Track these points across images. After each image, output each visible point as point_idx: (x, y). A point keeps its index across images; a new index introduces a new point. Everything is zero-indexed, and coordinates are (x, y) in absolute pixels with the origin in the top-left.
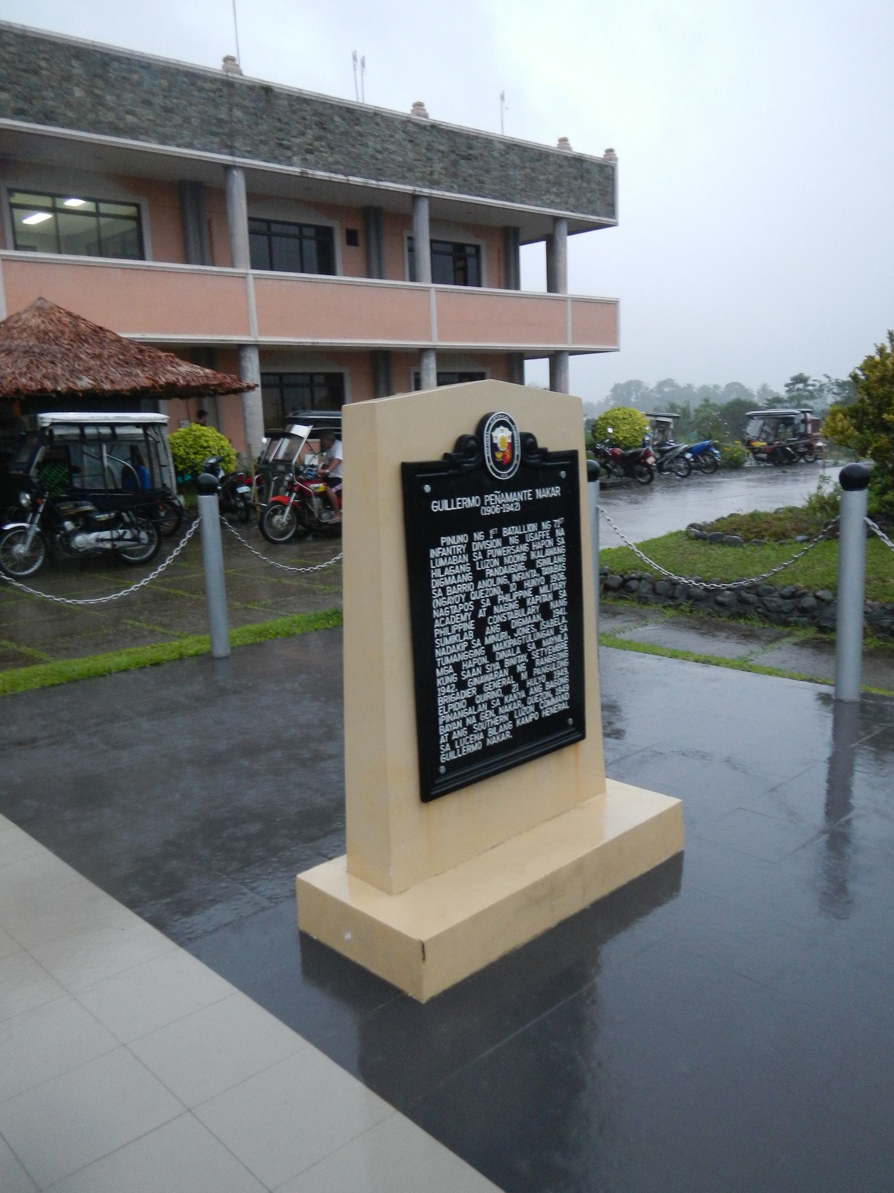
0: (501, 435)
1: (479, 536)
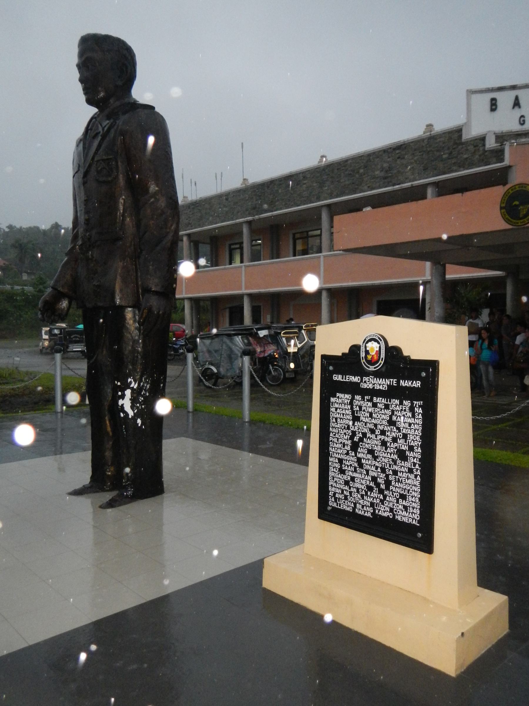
0: (373, 347)
1: (358, 397)
